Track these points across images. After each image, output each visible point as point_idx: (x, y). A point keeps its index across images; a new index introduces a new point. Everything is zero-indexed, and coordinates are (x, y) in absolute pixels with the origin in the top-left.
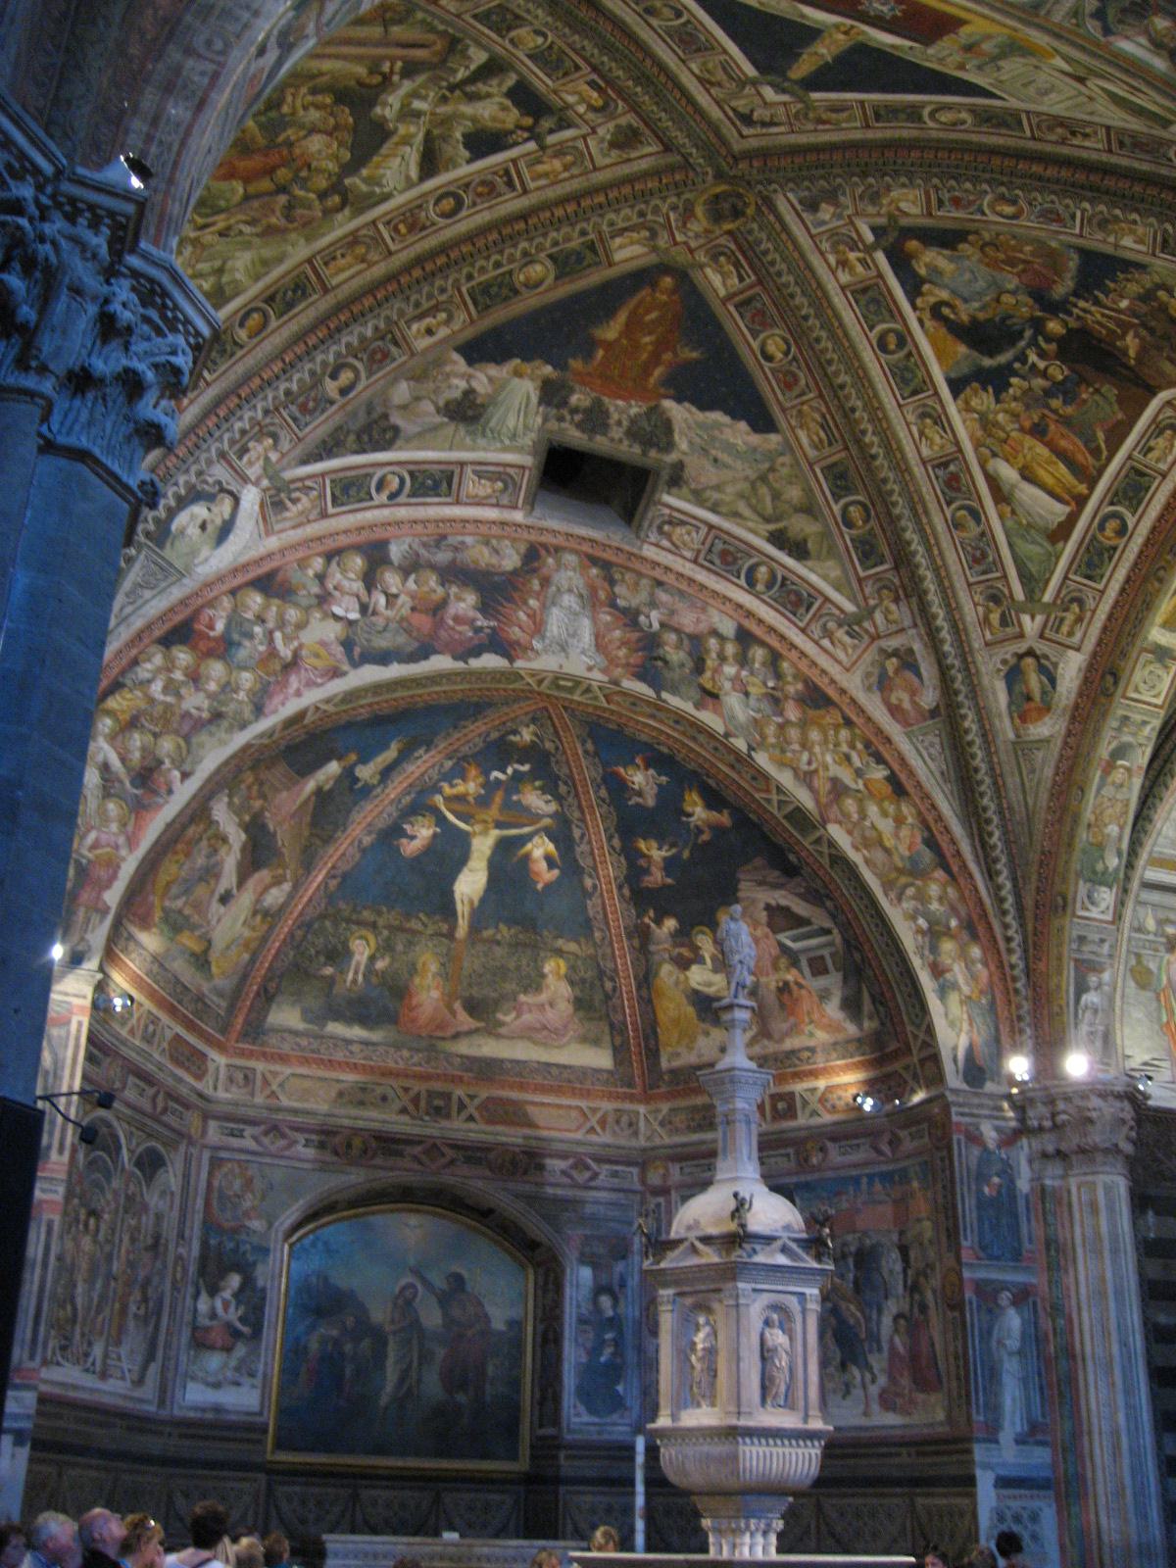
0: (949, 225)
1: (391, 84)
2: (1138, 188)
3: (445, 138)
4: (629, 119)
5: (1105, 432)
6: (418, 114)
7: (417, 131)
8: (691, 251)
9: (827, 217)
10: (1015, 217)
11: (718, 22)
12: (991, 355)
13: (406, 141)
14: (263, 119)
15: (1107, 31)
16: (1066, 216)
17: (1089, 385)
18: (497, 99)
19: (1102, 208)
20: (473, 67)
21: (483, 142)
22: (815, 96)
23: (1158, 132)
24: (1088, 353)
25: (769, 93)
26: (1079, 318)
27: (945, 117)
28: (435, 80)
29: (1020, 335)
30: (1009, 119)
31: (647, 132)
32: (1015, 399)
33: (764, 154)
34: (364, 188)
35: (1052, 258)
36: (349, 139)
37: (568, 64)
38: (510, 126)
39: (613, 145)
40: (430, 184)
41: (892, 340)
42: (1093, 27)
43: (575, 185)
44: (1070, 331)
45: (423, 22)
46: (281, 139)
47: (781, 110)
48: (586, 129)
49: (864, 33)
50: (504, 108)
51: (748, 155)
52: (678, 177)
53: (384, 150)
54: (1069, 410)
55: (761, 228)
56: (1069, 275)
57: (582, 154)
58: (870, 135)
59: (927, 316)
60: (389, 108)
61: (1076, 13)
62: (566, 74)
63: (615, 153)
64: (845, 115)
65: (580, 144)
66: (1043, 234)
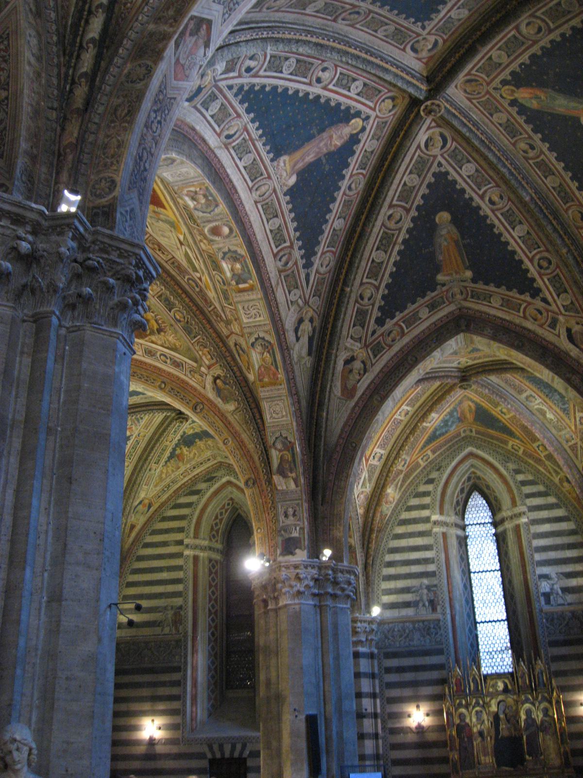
2: (169, 279)
15: (223, 258)
19: (168, 293)
23: (192, 273)
42: (220, 255)
61: (219, 249)
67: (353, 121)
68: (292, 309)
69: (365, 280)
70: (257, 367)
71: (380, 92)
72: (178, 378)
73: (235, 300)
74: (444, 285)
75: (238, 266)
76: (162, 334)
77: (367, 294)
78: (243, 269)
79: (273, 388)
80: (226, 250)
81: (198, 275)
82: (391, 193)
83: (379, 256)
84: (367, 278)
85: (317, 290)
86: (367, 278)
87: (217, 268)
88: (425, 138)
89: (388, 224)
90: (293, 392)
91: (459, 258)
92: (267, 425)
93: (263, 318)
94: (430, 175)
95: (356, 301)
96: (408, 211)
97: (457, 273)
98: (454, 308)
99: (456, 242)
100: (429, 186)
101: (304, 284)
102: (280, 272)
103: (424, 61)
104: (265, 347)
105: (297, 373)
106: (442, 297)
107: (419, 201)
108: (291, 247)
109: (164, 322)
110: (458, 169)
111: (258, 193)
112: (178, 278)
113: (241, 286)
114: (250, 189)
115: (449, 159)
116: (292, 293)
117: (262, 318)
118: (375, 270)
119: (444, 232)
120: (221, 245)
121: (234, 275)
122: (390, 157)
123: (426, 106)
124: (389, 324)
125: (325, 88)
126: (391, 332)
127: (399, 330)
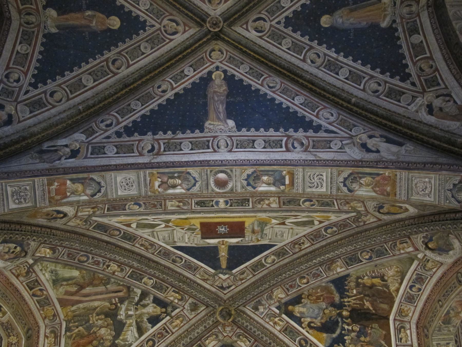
0: (295, 295)
1: (119, 308)
3: (142, 322)
4: (191, 300)
5: (383, 340)
6: (131, 316)
7: (132, 321)
8: (230, 337)
9: (262, 310)
10: (308, 282)
11: (191, 256)
12: (334, 332)
13: (131, 325)
14: (85, 326)
15: (254, 188)
16: (319, 273)
17: (368, 327)
18: (151, 305)
20: (139, 295)
21: (154, 320)
22: (234, 271)
24: (360, 316)
25: (221, 276)
26: (349, 306)
27: (269, 260)
28: (130, 303)
29: (337, 322)
30: (283, 251)
31: (199, 303)
32: (350, 344)
33: (232, 297)
34: (122, 343)
35: (325, 289)
36: (112, 327)
37: (164, 287)
38: (159, 313)
39: (192, 310)
40: (143, 338)
41: (303, 342)
42: (249, 188)
43: (186, 327)
44: (350, 312)
45: (115, 282)
46: (91, 332)
47: (229, 281)
48: (182, 308)
49: (227, 242)
50: (155, 308)
51: (228, 299)
52: (212, 313)
53: (125, 329)
54: (368, 339)
55: (242, 319)
56: (335, 292)
57: (184, 316)
58: (257, 277)
59: (308, 329)
60: (122, 315)
62: (166, 291)
63: (193, 313)
64: (245, 274)
65: (182, 313)
66: (318, 283)
67: (213, 77)
68: (347, 149)
69: (362, 87)
70: (374, 194)
71: (202, 58)
72: (436, 285)
73: (300, 191)
74: (394, 21)
75: (265, 178)
76: (386, 278)
77: (374, 86)
78: (267, 175)
79: (398, 185)
80: (245, 183)
81: (316, 223)
82: (293, 60)
83: (344, 73)
84: (360, 85)
85: (347, 127)
86: (360, 85)
87: (265, 196)
88: (254, 32)
89: (318, 64)
90: (423, 166)
91: (368, 8)
92: (434, 203)
93: (326, 173)
94: (285, 30)
95: (378, 97)
96: (311, 48)
97: (385, 10)
98: (426, 13)
99: (352, 11)
100: (294, 31)
101: (333, 135)
102: (306, 151)
103: (187, 28)
104: (354, 180)
105: (407, 159)
106: (408, 23)
107: (306, 39)
108: (289, 137)
109: (374, 272)
110: (284, 9)
111: (222, 147)
112: (329, 241)
113: (287, 182)
114: (215, 151)
115: (275, 16)
116: (331, 146)
117: (324, 174)
118: (355, 77)
119: (340, 21)
120: (239, 185)
121: (274, 184)
122: (257, 56)
123: (210, 27)
124: (412, 70)
125: (173, 89)
126: (421, 69)
127: (423, 61)
